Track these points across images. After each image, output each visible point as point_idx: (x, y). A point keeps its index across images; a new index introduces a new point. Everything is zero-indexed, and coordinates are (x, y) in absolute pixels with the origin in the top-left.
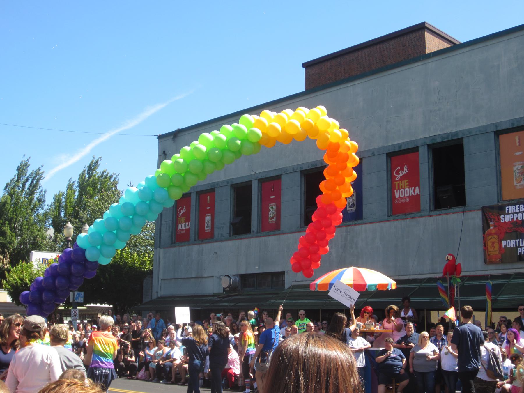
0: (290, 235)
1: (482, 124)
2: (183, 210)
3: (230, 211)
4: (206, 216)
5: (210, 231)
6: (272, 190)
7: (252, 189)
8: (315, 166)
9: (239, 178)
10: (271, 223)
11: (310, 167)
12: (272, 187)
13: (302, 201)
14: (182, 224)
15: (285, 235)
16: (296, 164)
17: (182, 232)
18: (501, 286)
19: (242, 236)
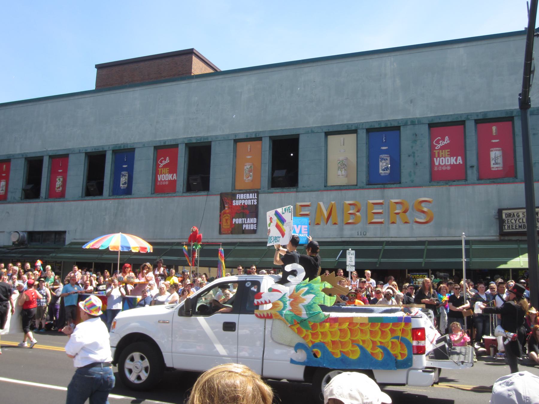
0: (72, 202)
1: (227, 133)
2: (166, 161)
3: (23, 179)
4: (492, 151)
5: (501, 169)
6: (125, 160)
7: (179, 154)
8: (97, 150)
9: (498, 111)
10: (246, 181)
11: (94, 151)
12: (384, 138)
13: (85, 177)
14: (164, 175)
15: (68, 202)
16: (81, 146)
17: (164, 183)
18: (230, 250)
19: (198, 194)
